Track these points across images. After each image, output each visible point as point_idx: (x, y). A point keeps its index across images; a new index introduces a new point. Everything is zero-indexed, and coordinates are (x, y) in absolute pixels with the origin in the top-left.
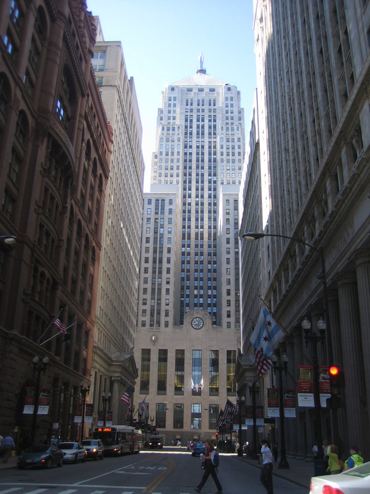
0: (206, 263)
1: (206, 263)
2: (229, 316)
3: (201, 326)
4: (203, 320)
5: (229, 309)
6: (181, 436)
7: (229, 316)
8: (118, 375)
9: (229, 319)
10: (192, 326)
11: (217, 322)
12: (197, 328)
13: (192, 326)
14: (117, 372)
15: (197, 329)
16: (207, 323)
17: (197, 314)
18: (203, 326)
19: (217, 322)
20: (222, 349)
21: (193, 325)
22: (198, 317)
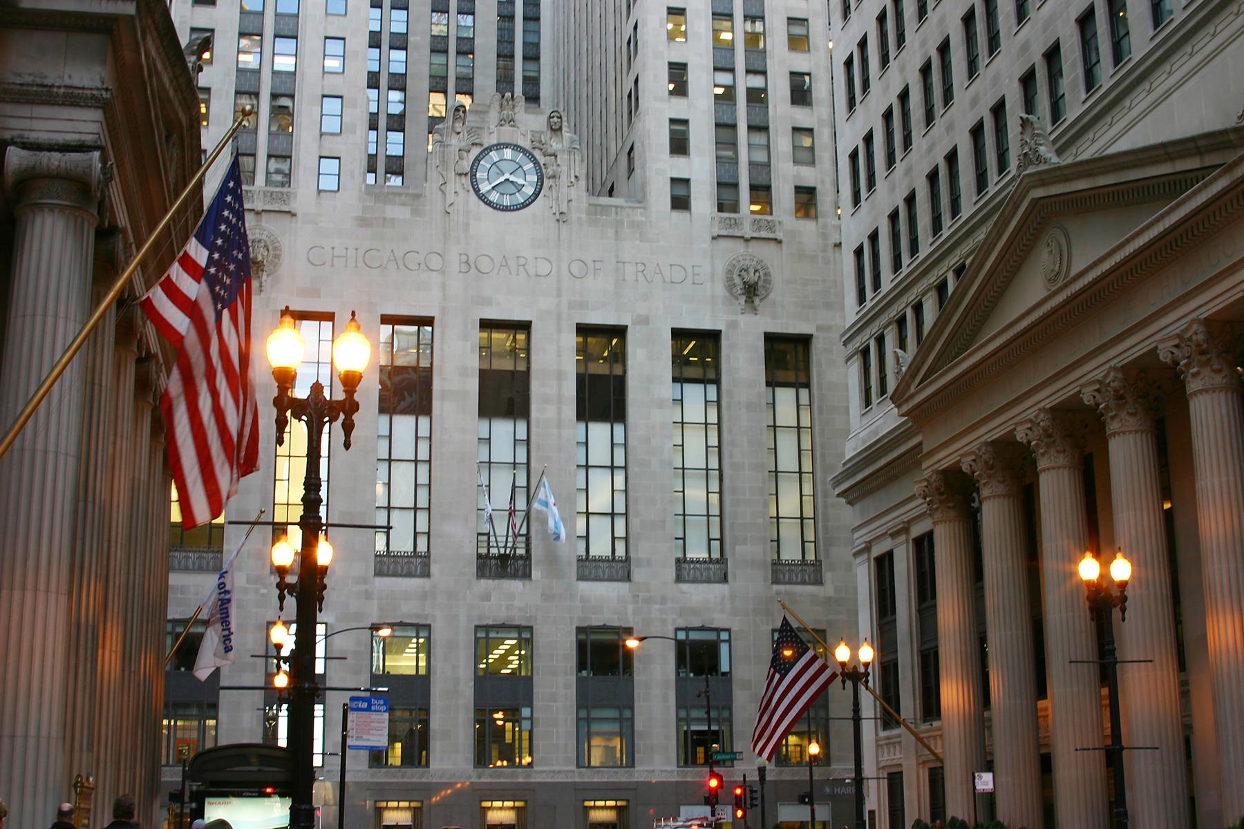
0: (419, 83)
1: (419, 83)
2: (679, 145)
3: (529, 191)
4: (536, 162)
5: (678, 108)
6: (417, 812)
7: (679, 145)
8: (85, 124)
9: (680, 160)
10: (477, 191)
11: (612, 178)
12: (507, 201)
13: (477, 191)
14: (73, 99)
15: (506, 209)
16: (564, 178)
17: (507, 128)
18: (536, 195)
19: (612, 178)
20: (644, 321)
21: (485, 188)
22: (507, 145)
